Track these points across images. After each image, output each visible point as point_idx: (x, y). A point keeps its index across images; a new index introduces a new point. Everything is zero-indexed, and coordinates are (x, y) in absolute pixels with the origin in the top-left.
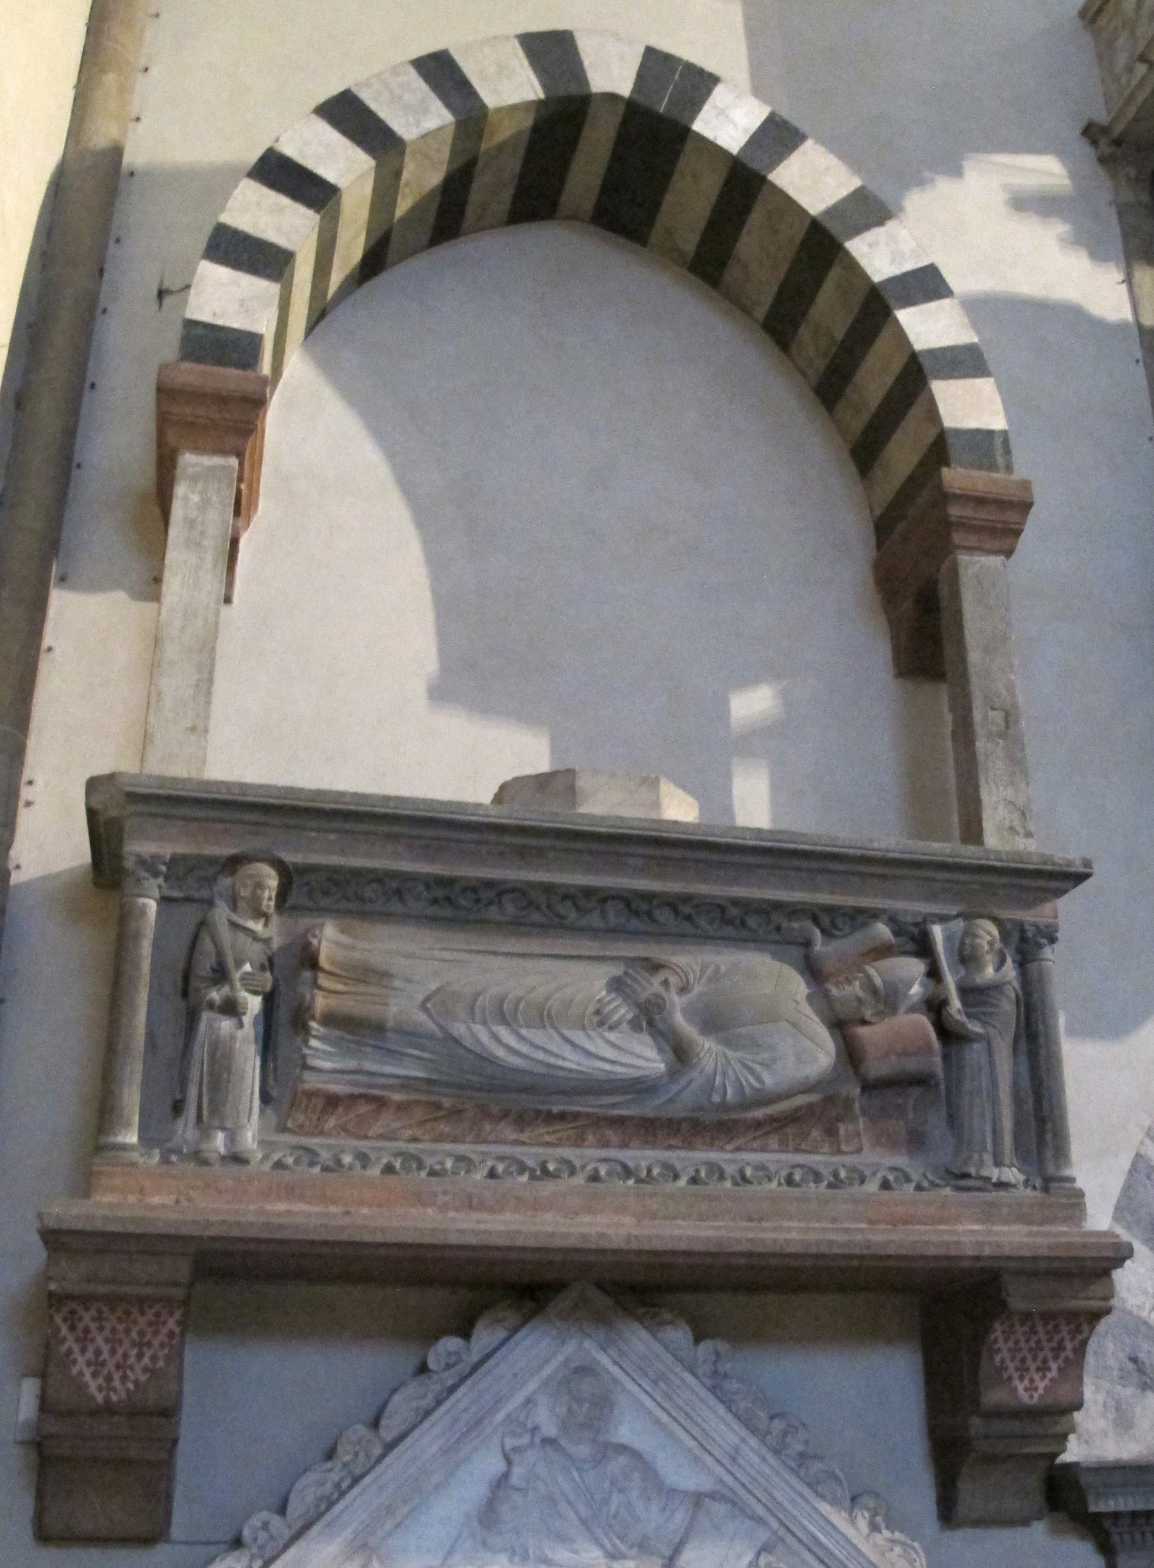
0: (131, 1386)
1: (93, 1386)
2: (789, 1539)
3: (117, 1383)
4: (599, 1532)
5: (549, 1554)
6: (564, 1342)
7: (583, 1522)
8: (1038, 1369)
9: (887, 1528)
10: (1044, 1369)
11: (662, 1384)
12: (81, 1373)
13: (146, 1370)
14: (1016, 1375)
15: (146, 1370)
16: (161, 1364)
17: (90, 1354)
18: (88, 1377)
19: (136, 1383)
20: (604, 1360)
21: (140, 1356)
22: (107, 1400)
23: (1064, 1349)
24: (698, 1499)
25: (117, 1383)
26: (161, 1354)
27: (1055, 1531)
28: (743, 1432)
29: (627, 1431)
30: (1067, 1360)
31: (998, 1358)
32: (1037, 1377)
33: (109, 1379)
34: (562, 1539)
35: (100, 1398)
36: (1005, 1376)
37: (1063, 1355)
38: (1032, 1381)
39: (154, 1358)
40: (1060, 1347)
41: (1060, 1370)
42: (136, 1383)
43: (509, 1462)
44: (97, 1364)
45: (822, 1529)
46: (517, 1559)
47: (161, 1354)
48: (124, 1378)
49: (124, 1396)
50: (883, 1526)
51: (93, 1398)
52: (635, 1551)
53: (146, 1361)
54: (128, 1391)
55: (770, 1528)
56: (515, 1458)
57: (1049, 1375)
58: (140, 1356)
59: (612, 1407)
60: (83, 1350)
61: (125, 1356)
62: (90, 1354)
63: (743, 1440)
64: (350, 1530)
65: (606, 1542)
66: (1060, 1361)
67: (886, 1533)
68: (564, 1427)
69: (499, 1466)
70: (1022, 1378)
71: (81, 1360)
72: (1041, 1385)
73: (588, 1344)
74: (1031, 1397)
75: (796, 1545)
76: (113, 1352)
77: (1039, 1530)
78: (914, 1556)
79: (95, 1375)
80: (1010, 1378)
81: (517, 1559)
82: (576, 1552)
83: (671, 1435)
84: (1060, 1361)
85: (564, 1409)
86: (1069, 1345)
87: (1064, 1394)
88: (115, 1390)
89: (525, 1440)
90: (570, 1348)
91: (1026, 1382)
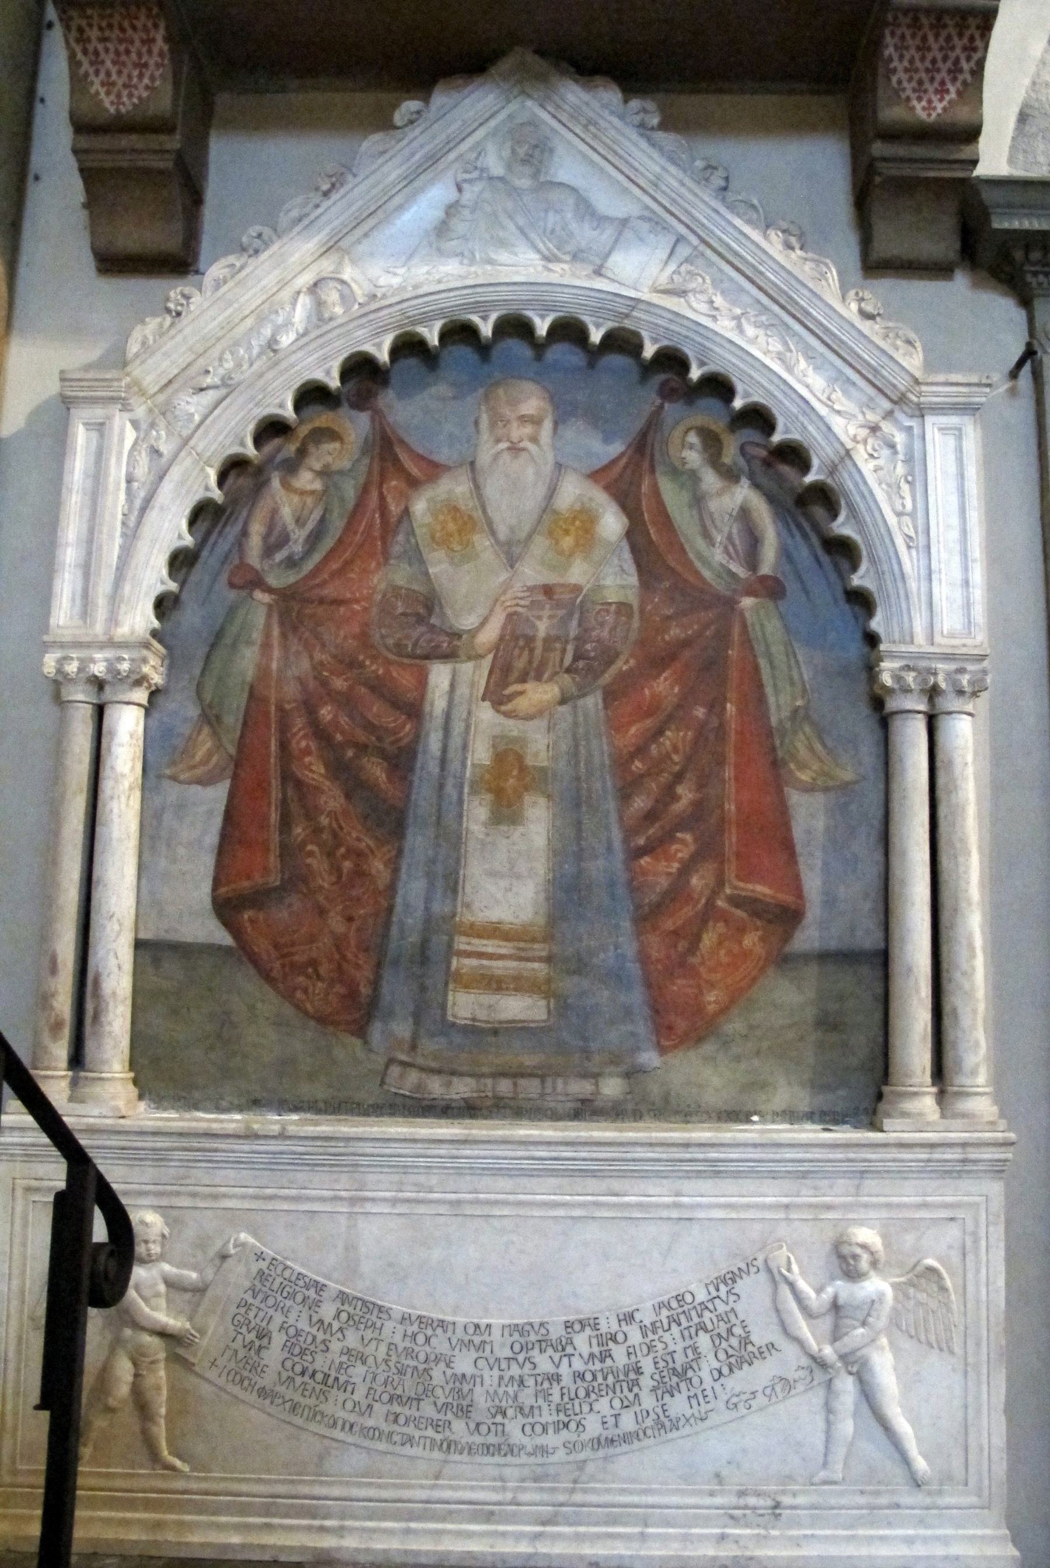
0: (135, 100)
1: (107, 104)
2: (709, 253)
3: (125, 99)
4: (533, 235)
5: (493, 256)
6: (508, 101)
7: (521, 230)
8: (937, 91)
9: (801, 249)
10: (942, 91)
11: (592, 128)
12: (97, 93)
13: (147, 87)
14: (913, 96)
15: (147, 87)
16: (158, 83)
17: (102, 76)
18: (103, 95)
19: (140, 98)
20: (544, 115)
21: (141, 76)
22: (118, 110)
23: (961, 71)
24: (624, 222)
25: (125, 99)
26: (157, 74)
27: (976, 285)
28: (663, 161)
29: (563, 175)
30: (965, 83)
31: (894, 79)
32: (935, 98)
33: (119, 96)
34: (502, 244)
35: (112, 110)
36: (903, 96)
37: (961, 77)
38: (930, 101)
39: (152, 78)
40: (955, 71)
41: (959, 93)
42: (140, 98)
43: (460, 189)
44: (108, 84)
45: (736, 240)
46: (465, 261)
47: (157, 74)
48: (130, 96)
49: (130, 108)
50: (797, 246)
51: (107, 110)
52: (567, 258)
53: (146, 81)
54: (134, 105)
55: (689, 243)
56: (465, 186)
57: (947, 98)
58: (141, 76)
59: (551, 151)
60: (97, 73)
61: (130, 77)
62: (102, 76)
63: (663, 168)
64: (324, 233)
65: (541, 246)
66: (958, 84)
67: (799, 252)
68: (509, 167)
69: (452, 195)
70: (919, 99)
71: (97, 81)
72: (940, 107)
73: (529, 103)
74: (929, 115)
75: (715, 258)
76: (120, 72)
77: (960, 282)
78: (825, 269)
79: (108, 93)
80: (908, 99)
81: (465, 261)
82: (516, 255)
83: (602, 170)
84: (958, 84)
85: (509, 151)
86: (965, 66)
87: (963, 115)
88: (123, 104)
89: (475, 174)
90: (513, 106)
91: (924, 103)
